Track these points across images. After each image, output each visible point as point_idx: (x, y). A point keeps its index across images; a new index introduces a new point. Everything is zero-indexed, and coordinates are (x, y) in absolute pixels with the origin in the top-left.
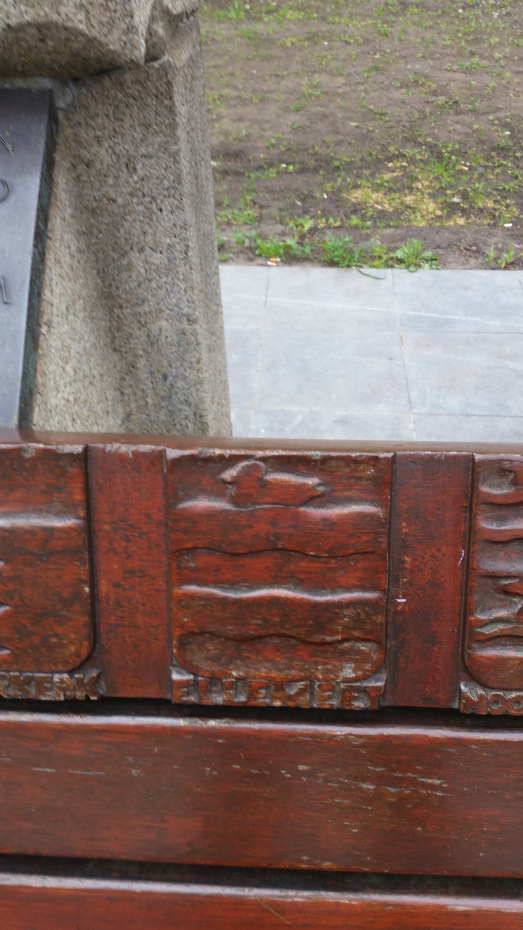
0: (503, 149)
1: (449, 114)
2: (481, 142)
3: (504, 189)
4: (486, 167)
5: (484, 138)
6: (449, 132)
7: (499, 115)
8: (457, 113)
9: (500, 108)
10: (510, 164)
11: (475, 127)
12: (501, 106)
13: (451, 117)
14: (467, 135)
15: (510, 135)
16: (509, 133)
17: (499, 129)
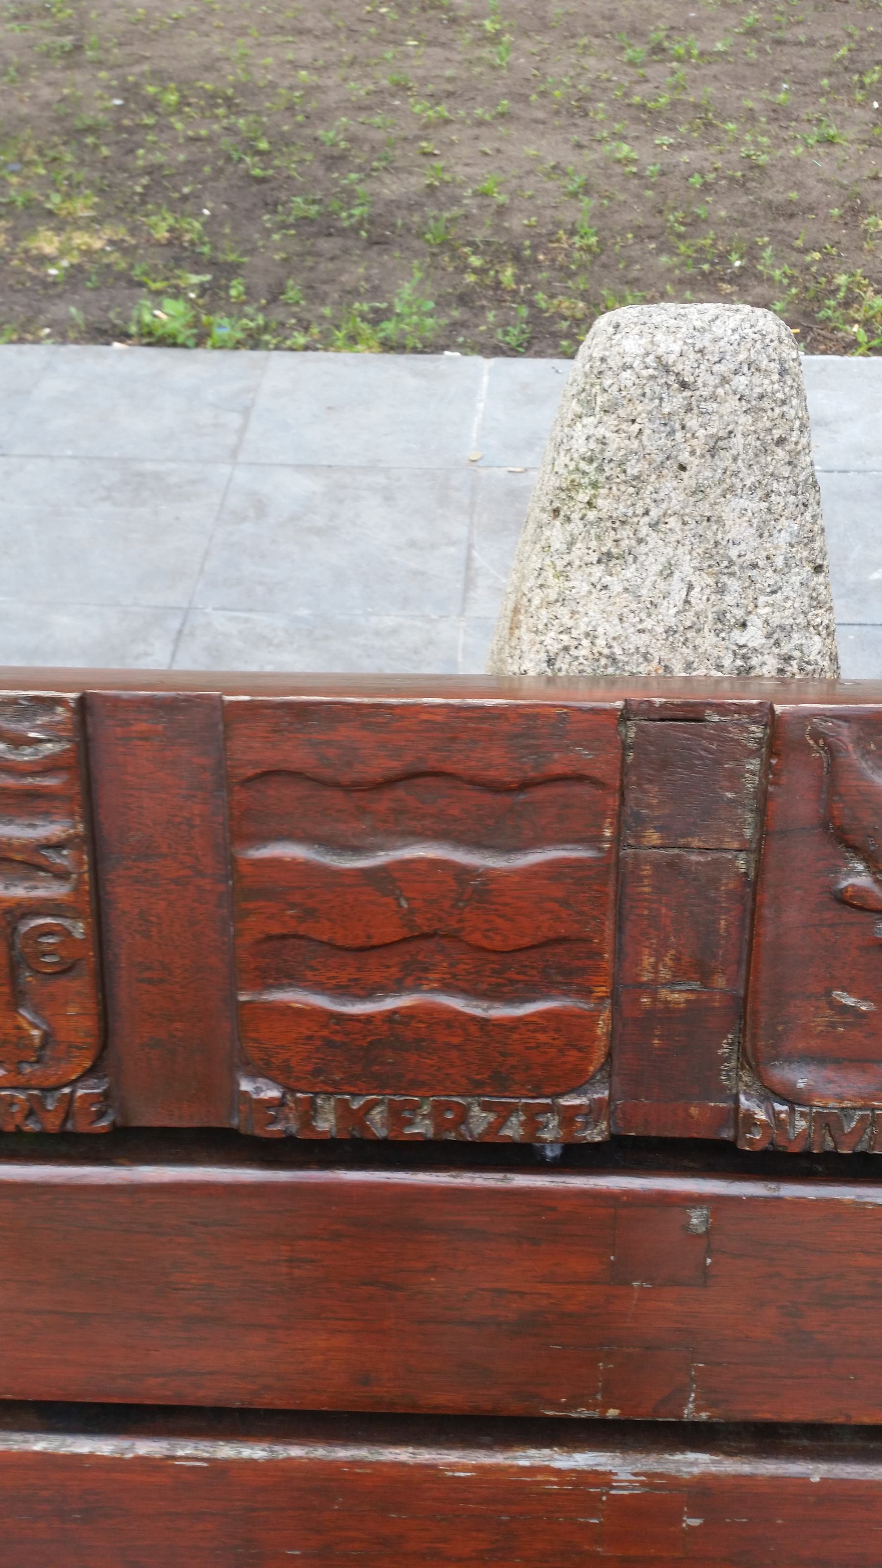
0: (90, 130)
1: (53, 68)
2: (58, 119)
3: (13, 202)
4: (30, 163)
5: (63, 109)
6: (21, 101)
7: (137, 69)
8: (66, 68)
9: (147, 58)
10: (68, 158)
11: (66, 91)
12: (148, 54)
13: (51, 75)
14: (48, 105)
15: (120, 107)
16: (118, 102)
17: (106, 96)
